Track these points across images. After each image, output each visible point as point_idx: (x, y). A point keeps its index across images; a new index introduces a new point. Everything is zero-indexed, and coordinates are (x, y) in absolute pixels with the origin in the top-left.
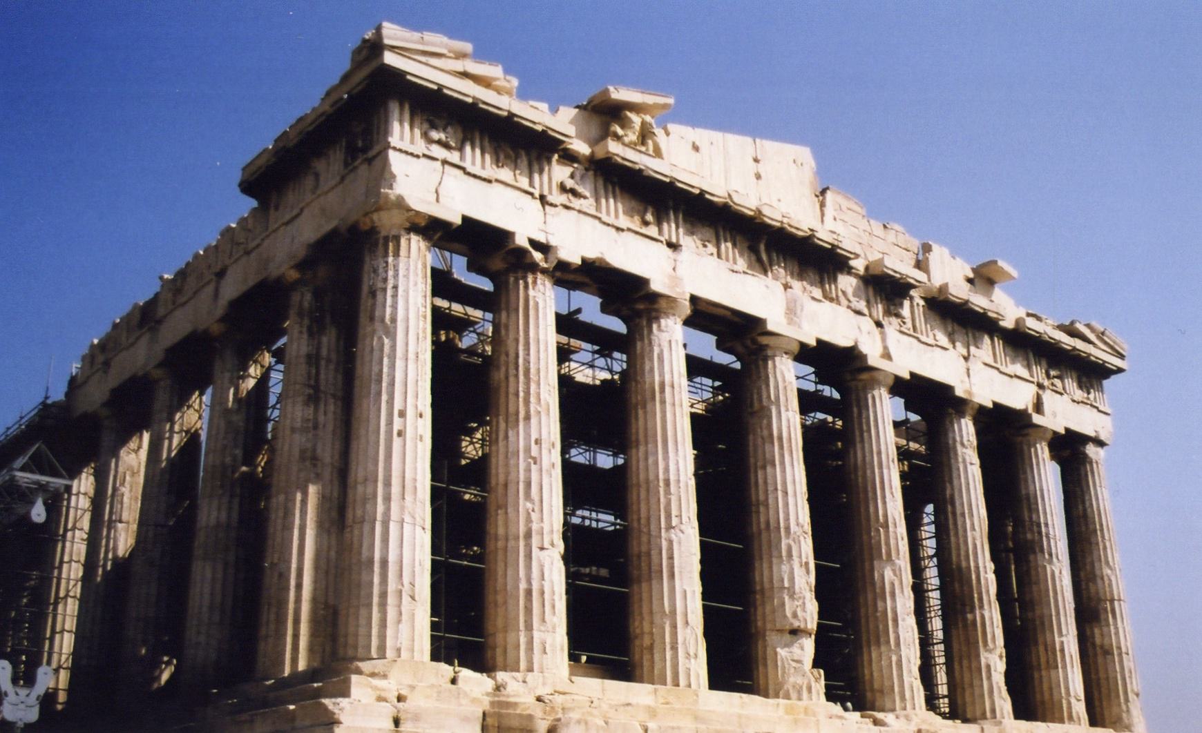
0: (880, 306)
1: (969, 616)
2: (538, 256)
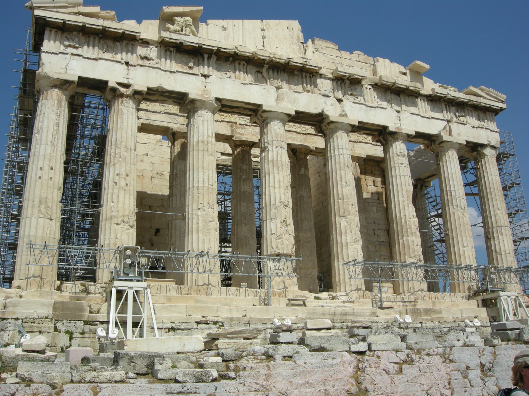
0: (340, 92)
2: (123, 90)
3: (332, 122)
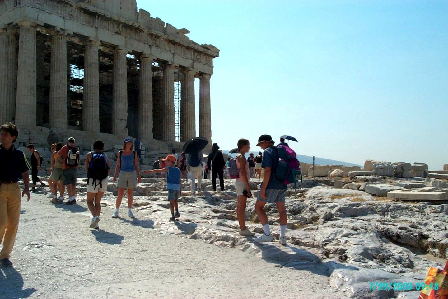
1: (167, 117)
2: (62, 32)
3: (146, 57)
